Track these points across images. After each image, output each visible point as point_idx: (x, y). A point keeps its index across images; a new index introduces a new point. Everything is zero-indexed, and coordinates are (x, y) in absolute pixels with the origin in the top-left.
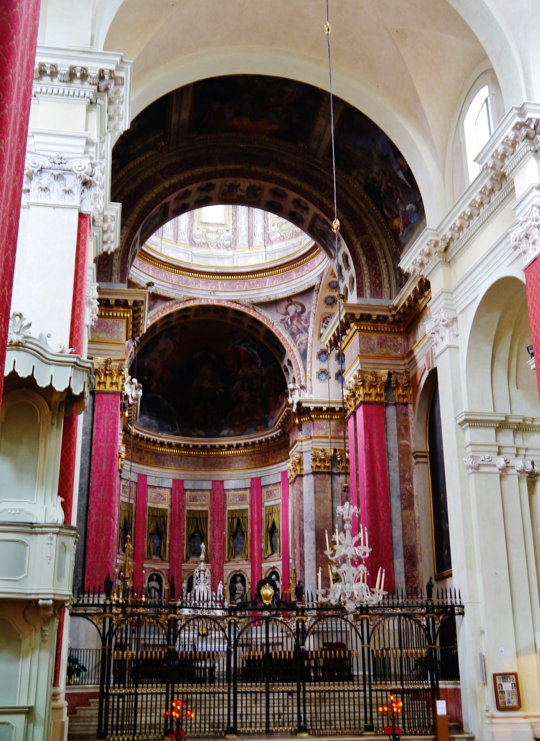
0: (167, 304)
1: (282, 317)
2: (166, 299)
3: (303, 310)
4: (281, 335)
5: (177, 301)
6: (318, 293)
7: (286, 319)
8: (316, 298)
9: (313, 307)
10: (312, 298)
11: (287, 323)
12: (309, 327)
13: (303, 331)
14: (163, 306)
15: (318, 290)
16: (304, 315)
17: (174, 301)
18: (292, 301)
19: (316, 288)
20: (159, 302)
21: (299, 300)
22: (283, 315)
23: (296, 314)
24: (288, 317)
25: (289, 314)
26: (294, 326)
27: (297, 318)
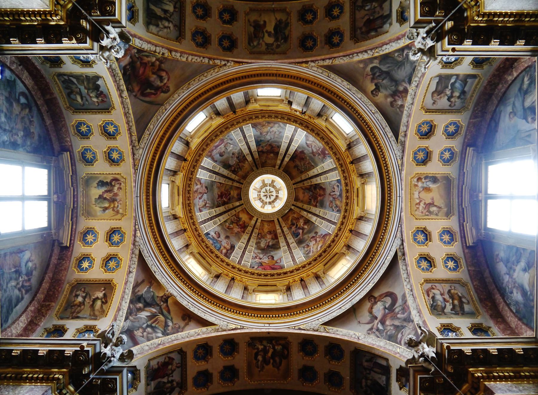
0: (204, 329)
1: (369, 326)
2: (204, 323)
3: (394, 300)
4: (374, 345)
5: (217, 327)
6: (404, 259)
7: (375, 326)
8: (404, 268)
9: (405, 283)
10: (399, 274)
11: (378, 330)
12: (410, 313)
13: (405, 324)
14: (197, 330)
15: (404, 254)
16: (397, 305)
17: (213, 327)
18: (375, 298)
19: (399, 254)
20: (192, 324)
21: (384, 290)
22: (368, 323)
23: (387, 311)
24: (376, 322)
25: (376, 318)
26: (389, 328)
27: (390, 315)
